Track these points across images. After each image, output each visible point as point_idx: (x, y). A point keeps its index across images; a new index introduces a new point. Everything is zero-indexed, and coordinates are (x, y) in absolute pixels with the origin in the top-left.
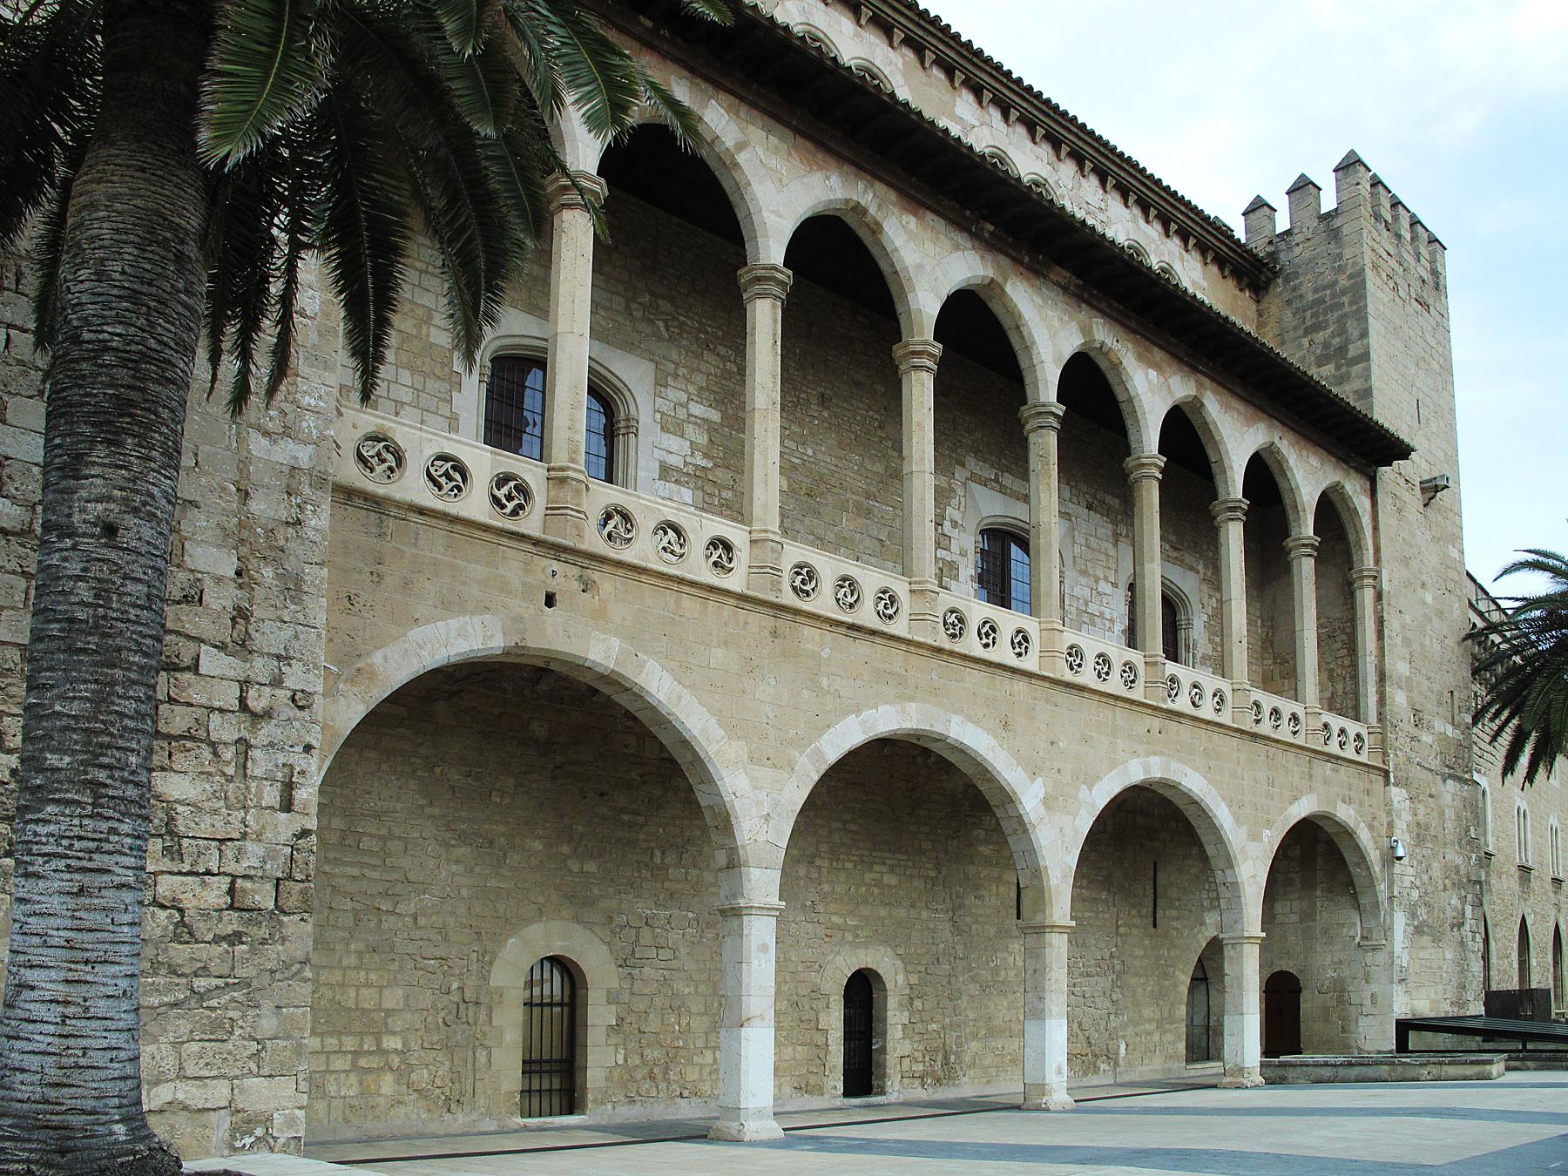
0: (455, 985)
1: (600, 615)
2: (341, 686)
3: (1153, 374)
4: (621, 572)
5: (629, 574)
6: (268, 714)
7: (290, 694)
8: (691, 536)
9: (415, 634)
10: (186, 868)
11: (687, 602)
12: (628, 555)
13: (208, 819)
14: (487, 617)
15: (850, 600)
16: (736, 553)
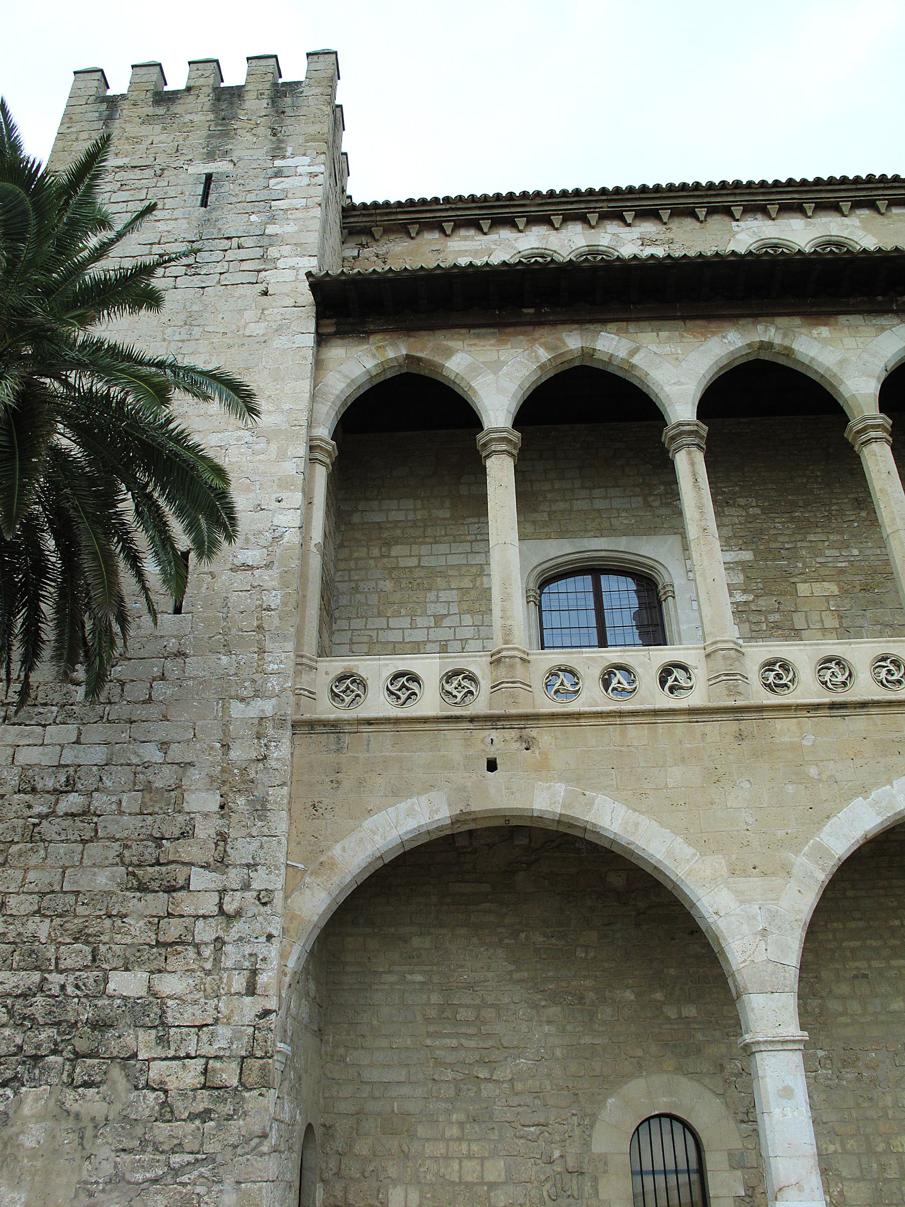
0: (557, 1154)
1: (542, 767)
2: (307, 880)
4: (559, 722)
5: (567, 722)
6: (238, 914)
7: (255, 894)
8: (639, 670)
9: (368, 823)
10: (171, 1053)
11: (632, 731)
12: (574, 706)
13: (190, 1010)
14: (433, 794)
15: (841, 678)
16: (693, 672)
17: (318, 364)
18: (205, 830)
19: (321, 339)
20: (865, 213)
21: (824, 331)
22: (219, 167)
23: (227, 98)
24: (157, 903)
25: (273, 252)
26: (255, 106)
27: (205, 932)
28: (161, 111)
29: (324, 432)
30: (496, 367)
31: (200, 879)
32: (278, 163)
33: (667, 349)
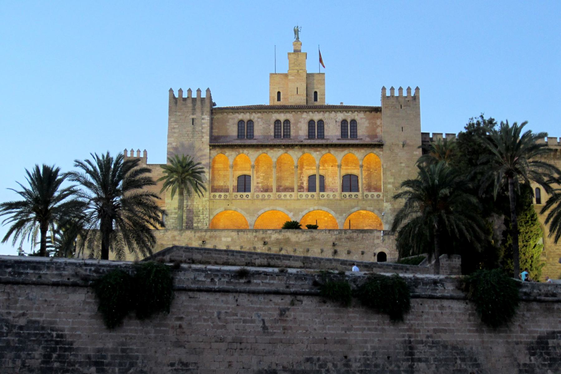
3: (318, 153)
17: (210, 153)
18: (201, 211)
19: (210, 150)
20: (293, 113)
21: (272, 151)
22: (194, 117)
23: (194, 100)
24: (197, 218)
25: (203, 135)
26: (199, 103)
27: (202, 220)
28: (184, 102)
30: (231, 155)
31: (201, 216)
32: (203, 117)
33: (253, 153)
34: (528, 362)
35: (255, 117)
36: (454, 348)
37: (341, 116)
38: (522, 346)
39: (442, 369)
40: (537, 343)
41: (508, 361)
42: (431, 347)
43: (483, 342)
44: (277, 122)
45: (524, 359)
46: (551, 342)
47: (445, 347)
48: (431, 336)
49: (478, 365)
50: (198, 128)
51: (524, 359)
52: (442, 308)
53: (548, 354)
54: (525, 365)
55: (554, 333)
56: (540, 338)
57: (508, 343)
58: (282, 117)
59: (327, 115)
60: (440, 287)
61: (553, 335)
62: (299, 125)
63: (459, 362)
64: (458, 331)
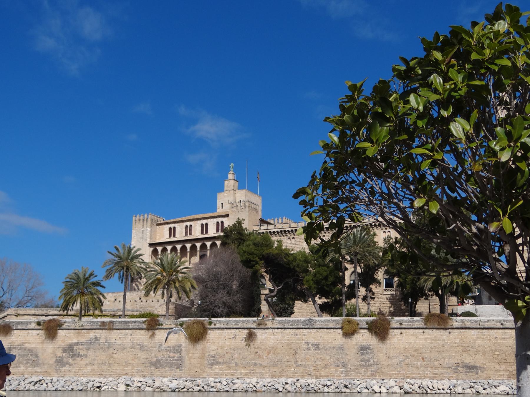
26: (145, 221)
29: (151, 254)
34: (61, 356)
35: (176, 225)
36: (29, 350)
37: (216, 220)
38: (60, 349)
39: (21, 359)
40: (69, 347)
41: (52, 355)
42: (19, 350)
43: (43, 348)
44: (187, 226)
45: (59, 354)
46: (75, 347)
47: (25, 349)
48: (20, 345)
49: (37, 357)
50: (145, 235)
51: (59, 354)
52: (29, 333)
53: (72, 352)
54: (60, 357)
55: (78, 343)
56: (70, 345)
57: (54, 348)
58: (188, 224)
59: (209, 220)
60: (29, 325)
61: (77, 344)
62: (196, 227)
63: (29, 356)
64: (33, 343)
